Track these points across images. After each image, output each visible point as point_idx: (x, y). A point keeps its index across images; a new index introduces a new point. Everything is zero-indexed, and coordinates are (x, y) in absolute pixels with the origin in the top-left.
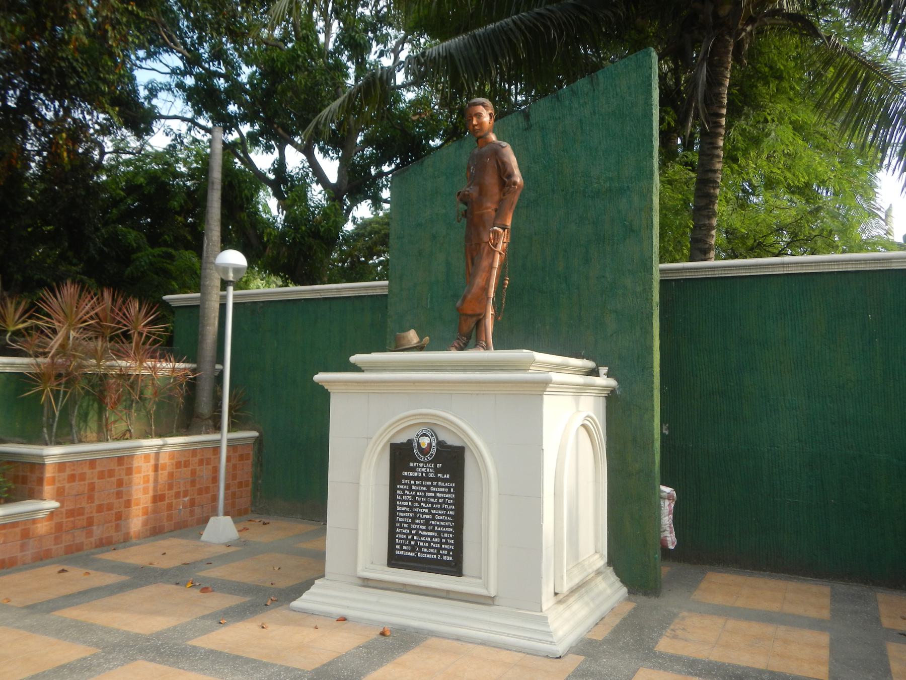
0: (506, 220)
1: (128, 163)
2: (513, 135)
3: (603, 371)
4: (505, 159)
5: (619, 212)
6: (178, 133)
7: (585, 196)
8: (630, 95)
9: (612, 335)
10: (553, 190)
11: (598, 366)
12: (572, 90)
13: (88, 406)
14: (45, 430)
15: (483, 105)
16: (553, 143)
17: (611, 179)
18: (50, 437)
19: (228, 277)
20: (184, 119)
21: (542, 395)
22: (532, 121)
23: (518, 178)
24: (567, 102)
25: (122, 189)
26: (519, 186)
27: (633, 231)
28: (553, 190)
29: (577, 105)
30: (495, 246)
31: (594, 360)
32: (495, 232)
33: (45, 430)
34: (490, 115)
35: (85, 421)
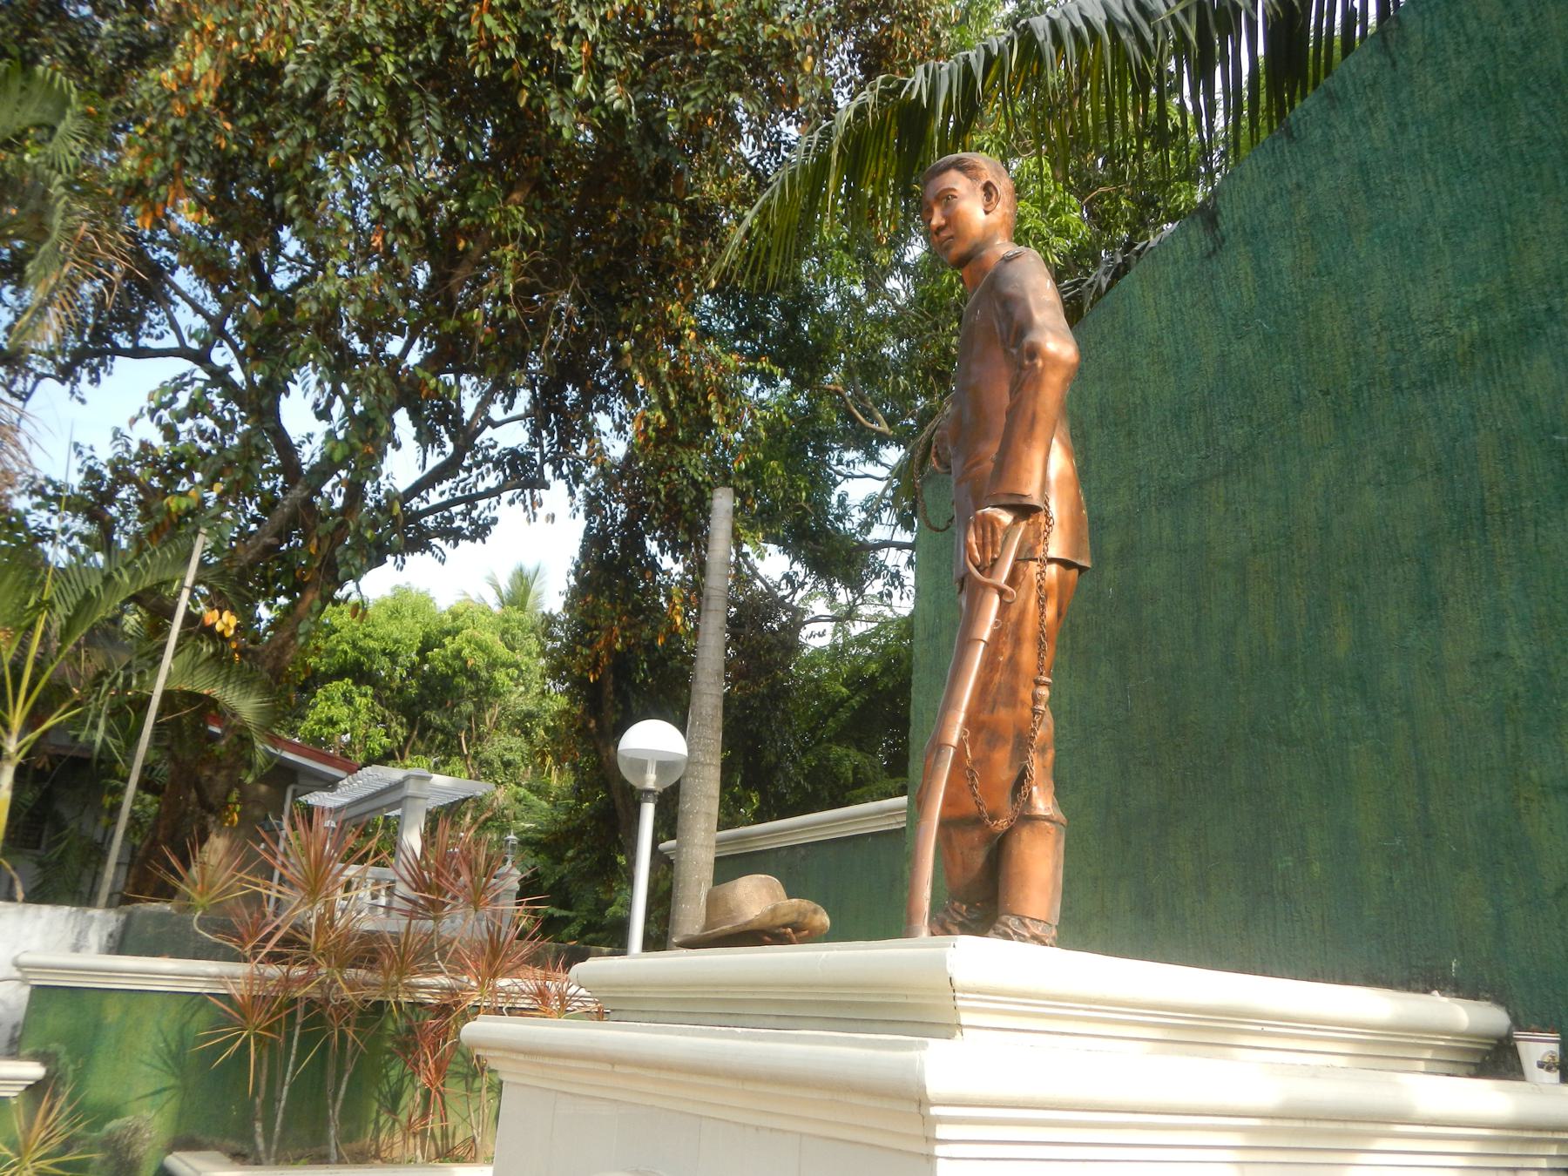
0: (1017, 481)
1: (862, 640)
2: (1178, 285)
3: (1537, 1049)
4: (1010, 290)
5: (1527, 405)
6: (893, 570)
7: (1399, 388)
8: (1516, 19)
10: (1297, 402)
11: (1517, 1023)
12: (1331, 96)
13: (401, 1080)
14: (259, 1127)
15: (960, 166)
16: (1286, 261)
17: (1485, 306)
18: (268, 1140)
19: (644, 782)
20: (901, 546)
21: (931, 1158)
22: (1225, 225)
23: (1056, 342)
24: (1318, 132)
25: (845, 684)
26: (1054, 361)
28: (1297, 402)
30: (989, 567)
31: (1498, 997)
32: (989, 524)
33: (259, 1127)
34: (988, 189)
35: (393, 1110)
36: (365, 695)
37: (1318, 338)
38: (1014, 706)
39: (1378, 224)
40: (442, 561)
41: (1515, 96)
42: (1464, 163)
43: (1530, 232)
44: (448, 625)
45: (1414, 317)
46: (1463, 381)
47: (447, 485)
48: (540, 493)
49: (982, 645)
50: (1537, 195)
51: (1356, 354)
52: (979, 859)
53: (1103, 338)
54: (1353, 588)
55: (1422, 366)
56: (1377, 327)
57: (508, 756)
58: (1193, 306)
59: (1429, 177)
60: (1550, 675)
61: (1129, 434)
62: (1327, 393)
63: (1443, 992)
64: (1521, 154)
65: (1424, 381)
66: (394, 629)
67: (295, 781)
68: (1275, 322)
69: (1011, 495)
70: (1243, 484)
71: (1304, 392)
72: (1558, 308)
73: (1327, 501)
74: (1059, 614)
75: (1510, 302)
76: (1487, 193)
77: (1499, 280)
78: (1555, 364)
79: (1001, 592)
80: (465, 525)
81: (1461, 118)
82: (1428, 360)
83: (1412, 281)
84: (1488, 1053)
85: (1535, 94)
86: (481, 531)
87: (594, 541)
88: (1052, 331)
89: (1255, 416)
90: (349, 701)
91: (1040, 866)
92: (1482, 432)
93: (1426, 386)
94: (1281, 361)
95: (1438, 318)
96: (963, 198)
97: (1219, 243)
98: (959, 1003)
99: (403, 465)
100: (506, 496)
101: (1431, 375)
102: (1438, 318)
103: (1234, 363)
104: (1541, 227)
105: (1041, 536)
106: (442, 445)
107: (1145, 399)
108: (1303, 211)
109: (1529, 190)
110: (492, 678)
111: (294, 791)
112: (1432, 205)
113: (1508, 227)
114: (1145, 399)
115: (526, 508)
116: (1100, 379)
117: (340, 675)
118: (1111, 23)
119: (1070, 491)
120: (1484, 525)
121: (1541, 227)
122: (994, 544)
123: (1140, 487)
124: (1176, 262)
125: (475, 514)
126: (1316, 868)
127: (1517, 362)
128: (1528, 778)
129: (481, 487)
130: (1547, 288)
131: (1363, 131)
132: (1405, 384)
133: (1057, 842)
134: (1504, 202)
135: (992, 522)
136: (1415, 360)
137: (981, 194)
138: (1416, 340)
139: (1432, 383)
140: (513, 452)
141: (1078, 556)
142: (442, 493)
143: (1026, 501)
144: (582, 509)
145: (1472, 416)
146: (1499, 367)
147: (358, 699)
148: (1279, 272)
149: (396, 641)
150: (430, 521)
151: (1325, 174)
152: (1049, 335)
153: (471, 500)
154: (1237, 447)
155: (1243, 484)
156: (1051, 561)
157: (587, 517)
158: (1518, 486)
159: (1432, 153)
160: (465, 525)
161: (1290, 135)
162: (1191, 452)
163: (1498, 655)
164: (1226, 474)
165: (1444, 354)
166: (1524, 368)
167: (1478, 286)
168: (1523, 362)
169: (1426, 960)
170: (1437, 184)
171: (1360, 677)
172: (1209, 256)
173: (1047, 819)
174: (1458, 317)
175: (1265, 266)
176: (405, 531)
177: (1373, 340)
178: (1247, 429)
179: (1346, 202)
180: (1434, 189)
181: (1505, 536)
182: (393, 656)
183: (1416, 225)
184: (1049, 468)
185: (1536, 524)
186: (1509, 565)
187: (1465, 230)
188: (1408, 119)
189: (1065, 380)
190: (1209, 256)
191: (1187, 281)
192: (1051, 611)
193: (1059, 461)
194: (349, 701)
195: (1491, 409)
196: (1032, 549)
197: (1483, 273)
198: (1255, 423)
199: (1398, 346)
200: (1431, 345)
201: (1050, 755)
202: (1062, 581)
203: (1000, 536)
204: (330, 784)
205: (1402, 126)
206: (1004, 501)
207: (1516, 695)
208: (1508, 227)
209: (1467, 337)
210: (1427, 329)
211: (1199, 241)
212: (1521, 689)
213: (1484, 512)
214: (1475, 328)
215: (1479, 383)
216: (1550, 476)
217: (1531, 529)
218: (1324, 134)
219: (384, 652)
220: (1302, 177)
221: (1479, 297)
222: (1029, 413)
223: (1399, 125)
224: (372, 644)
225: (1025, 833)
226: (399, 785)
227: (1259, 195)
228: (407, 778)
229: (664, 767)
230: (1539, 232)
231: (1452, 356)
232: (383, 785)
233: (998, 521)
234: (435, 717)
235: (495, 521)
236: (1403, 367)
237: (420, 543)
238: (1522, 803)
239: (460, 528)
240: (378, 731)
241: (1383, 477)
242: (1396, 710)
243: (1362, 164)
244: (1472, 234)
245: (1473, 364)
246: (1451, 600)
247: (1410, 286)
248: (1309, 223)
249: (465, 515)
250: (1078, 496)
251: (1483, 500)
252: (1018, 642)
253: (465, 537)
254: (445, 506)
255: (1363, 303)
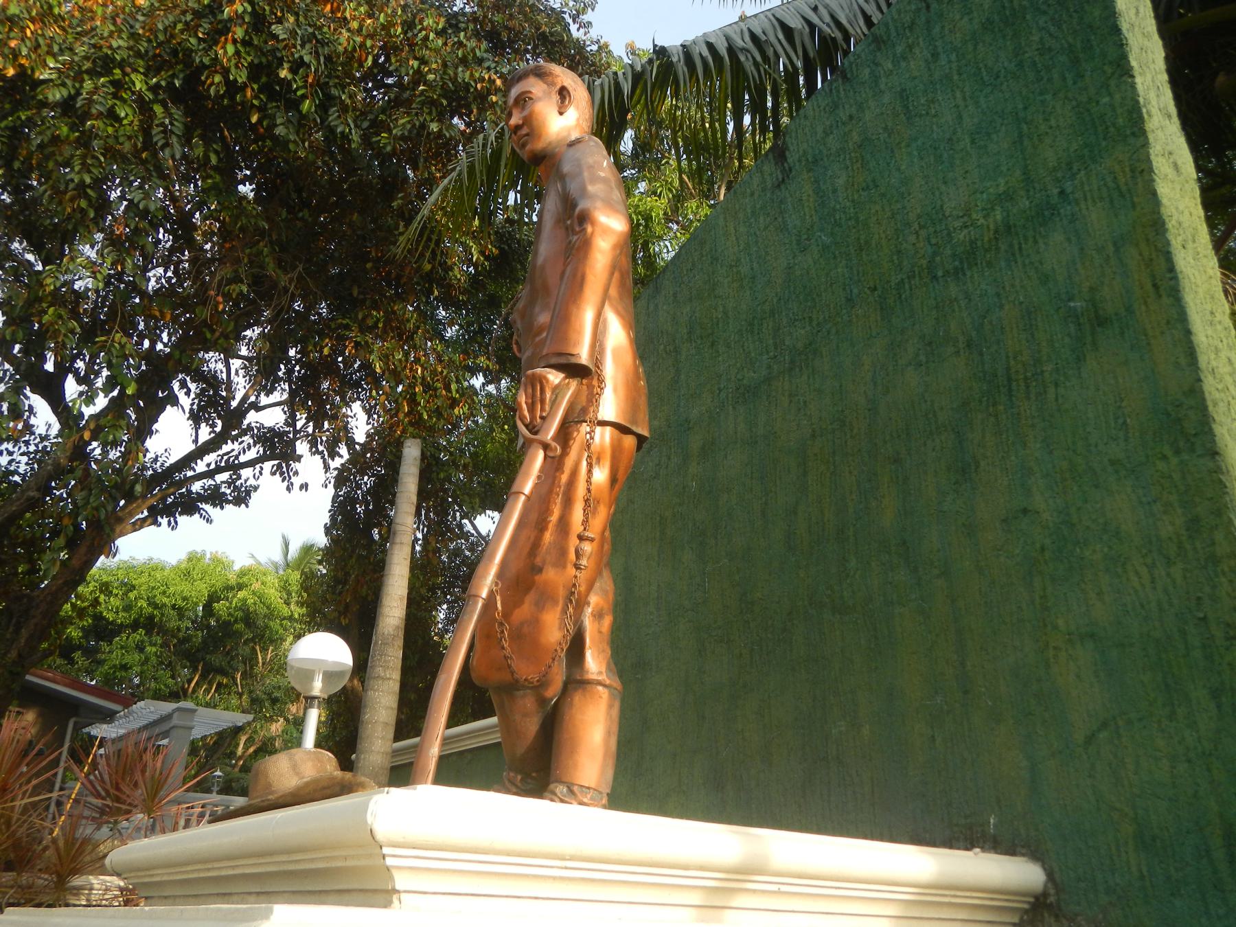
2: (753, 213)
5: (1045, 279)
7: (935, 278)
9: (1090, 739)
15: (540, 74)
16: (841, 182)
17: (1007, 197)
19: (311, 689)
22: (792, 157)
24: (867, 71)
26: (607, 230)
27: (1101, 321)
28: (849, 300)
29: (890, 66)
34: (563, 93)
36: (155, 645)
37: (867, 242)
38: (564, 567)
39: (916, 139)
40: (209, 521)
41: (1028, 17)
42: (986, 78)
43: (1043, 127)
44: (233, 582)
45: (947, 214)
46: (989, 265)
47: (211, 458)
48: (295, 466)
49: (523, 498)
50: (1048, 97)
51: (899, 252)
52: (531, 727)
53: (693, 265)
54: (897, 460)
55: (954, 255)
56: (916, 226)
57: (276, 694)
58: (766, 228)
59: (958, 94)
60: (1073, 525)
61: (712, 345)
62: (875, 289)
63: (984, 849)
64: (1034, 64)
65: (956, 269)
66: (184, 588)
67: (76, 715)
68: (832, 234)
69: (560, 354)
70: (805, 377)
71: (855, 291)
72: (1069, 190)
73: (875, 384)
74: (613, 479)
75: (1028, 191)
76: (1006, 100)
77: (1018, 173)
78: (1069, 240)
79: (546, 447)
80: (228, 491)
81: (984, 42)
82: (960, 250)
83: (945, 183)
84: (1026, 911)
85: (1045, 13)
86: (242, 497)
87: (342, 510)
88: (603, 201)
89: (814, 316)
90: (140, 648)
91: (594, 729)
92: (1007, 307)
93: (958, 273)
94: (836, 267)
95: (967, 213)
96: (540, 99)
97: (787, 174)
98: (389, 861)
99: (172, 436)
100: (268, 466)
101: (961, 262)
102: (967, 213)
103: (798, 273)
104: (1053, 122)
105: (593, 398)
106: (213, 426)
107: (725, 313)
108: (855, 137)
109: (1041, 94)
110: (267, 627)
111: (75, 723)
112: (960, 117)
113: (1025, 127)
114: (725, 313)
115: (283, 481)
116: (690, 300)
117: (135, 626)
118: (731, 50)
119: (628, 358)
120: (1010, 390)
121: (1053, 122)
122: (543, 401)
123: (720, 390)
124: (752, 194)
125: (238, 483)
126: (866, 731)
127: (1036, 242)
128: (1056, 627)
129: (243, 459)
130: (1059, 175)
131: (903, 64)
132: (940, 273)
133: (610, 706)
134: (1021, 106)
135: (542, 380)
136: (948, 252)
137: (556, 98)
138: (949, 234)
139: (962, 269)
140: (271, 430)
141: (634, 422)
142: (208, 465)
143: (573, 360)
144: (333, 481)
145: (998, 295)
146: (1020, 249)
147: (148, 649)
148: (835, 191)
149: (185, 599)
150: (197, 487)
151: (872, 104)
152: (599, 204)
153: (234, 467)
154: (800, 345)
155: (805, 377)
156: (603, 423)
157: (336, 487)
158: (1039, 352)
159: (960, 74)
160: (228, 491)
161: (844, 76)
162: (761, 354)
163: (1025, 511)
164: (791, 370)
165: (972, 242)
166: (1042, 246)
167: (1002, 181)
168: (1041, 241)
169: (966, 817)
170: (964, 99)
171: (904, 543)
172: (779, 186)
173: (600, 683)
174: (983, 209)
175: (823, 187)
176: (172, 495)
177: (912, 239)
178: (808, 328)
179: (890, 124)
180: (961, 103)
181: (1028, 398)
182: (180, 612)
183: (947, 136)
184: (603, 332)
185: (1057, 385)
186: (1033, 426)
187: (988, 134)
188: (940, 50)
189: (615, 247)
190: (779, 186)
191: (761, 208)
192: (601, 475)
193: (617, 335)
194: (140, 648)
195: (1013, 286)
196: (584, 411)
197: (1004, 169)
198: (815, 323)
199: (934, 241)
200: (961, 237)
201: (607, 621)
202: (616, 449)
203: (548, 395)
204: (108, 717)
205: (935, 56)
206: (554, 361)
207: (1043, 549)
208: (1025, 127)
209: (992, 227)
210: (958, 224)
211: (771, 175)
212: (1048, 541)
213: (1009, 380)
214: (999, 217)
215: (1003, 264)
216: (1067, 340)
217: (1052, 390)
218: (872, 72)
219: (173, 607)
220: (853, 110)
221: (1001, 189)
222: (579, 275)
223: (933, 55)
224: (165, 600)
225: (577, 698)
226: (168, 717)
227: (820, 129)
228: (174, 711)
229: (329, 676)
230: (1051, 127)
231: (979, 243)
232: (156, 717)
233: (547, 381)
234: (216, 659)
235: (256, 488)
236: (938, 259)
237: (190, 506)
238: (1051, 652)
239: (224, 494)
240: (164, 674)
241: (923, 358)
242: (936, 572)
243: (904, 90)
244: (994, 136)
245: (998, 249)
246: (982, 463)
247: (943, 188)
248: (860, 146)
249: (229, 483)
250: (636, 368)
251: (1008, 369)
252: (568, 502)
253: (229, 502)
254: (210, 474)
255: (904, 208)
